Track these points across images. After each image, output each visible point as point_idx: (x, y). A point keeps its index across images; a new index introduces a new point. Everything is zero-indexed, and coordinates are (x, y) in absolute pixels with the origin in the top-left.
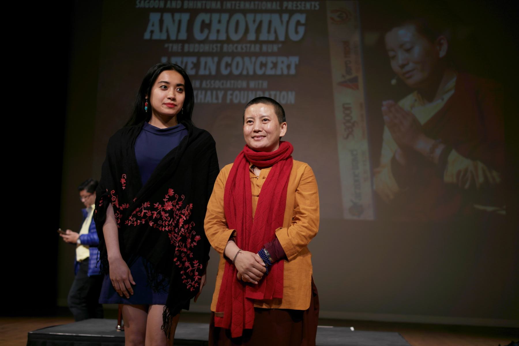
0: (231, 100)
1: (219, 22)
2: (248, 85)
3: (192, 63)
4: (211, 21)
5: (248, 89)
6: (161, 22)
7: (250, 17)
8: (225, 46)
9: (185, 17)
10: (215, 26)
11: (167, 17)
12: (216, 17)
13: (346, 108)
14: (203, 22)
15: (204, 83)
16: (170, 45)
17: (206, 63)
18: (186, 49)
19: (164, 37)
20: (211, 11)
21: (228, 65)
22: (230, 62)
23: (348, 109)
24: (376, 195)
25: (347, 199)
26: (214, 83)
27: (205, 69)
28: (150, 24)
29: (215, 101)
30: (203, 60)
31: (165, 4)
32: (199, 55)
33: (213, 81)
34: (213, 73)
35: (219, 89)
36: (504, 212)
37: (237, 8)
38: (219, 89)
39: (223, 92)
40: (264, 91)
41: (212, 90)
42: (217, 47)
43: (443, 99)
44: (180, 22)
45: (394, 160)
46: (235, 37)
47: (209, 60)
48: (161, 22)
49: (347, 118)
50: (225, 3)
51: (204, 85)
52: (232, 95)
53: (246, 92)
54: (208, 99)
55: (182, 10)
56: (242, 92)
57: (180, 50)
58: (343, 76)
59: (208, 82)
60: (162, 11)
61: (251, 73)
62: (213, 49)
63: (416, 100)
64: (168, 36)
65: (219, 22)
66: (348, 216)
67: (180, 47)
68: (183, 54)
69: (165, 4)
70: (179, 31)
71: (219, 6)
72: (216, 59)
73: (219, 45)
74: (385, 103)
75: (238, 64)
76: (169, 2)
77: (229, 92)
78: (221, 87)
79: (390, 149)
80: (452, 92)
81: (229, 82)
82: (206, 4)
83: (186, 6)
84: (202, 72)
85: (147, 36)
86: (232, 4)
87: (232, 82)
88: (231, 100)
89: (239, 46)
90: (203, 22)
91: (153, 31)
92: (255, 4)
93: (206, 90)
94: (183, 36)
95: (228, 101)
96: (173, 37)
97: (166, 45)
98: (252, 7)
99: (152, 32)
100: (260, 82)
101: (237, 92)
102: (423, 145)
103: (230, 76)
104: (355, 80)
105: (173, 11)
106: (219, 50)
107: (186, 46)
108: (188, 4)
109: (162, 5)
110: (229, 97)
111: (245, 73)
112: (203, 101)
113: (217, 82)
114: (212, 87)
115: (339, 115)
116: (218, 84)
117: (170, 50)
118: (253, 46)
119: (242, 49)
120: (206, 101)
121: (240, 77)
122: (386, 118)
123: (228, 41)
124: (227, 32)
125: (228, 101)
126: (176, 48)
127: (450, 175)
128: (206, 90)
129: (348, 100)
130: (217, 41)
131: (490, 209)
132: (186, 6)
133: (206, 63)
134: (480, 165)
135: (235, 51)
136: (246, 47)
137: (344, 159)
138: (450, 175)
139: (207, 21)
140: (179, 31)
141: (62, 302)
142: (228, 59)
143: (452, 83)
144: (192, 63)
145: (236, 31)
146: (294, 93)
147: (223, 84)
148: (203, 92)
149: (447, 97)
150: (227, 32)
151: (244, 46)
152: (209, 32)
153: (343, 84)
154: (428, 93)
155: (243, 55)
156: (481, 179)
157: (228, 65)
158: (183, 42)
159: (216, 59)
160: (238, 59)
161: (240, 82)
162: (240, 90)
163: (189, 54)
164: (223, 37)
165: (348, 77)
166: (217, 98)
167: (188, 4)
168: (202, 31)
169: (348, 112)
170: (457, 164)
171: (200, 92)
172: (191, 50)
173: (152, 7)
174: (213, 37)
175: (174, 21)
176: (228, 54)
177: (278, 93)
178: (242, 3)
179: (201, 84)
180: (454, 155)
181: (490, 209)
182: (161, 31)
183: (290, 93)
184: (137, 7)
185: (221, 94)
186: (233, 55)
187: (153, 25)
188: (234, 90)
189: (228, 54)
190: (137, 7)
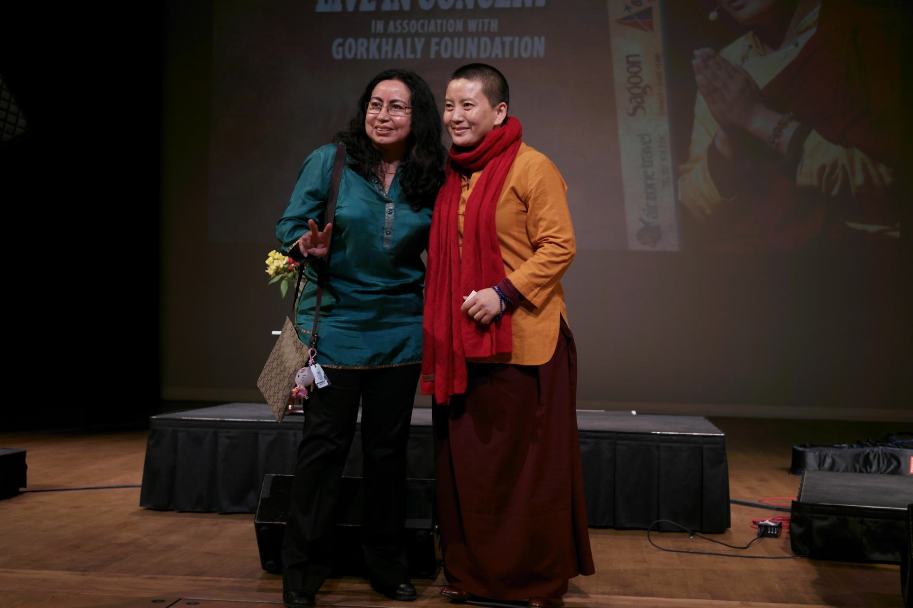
0: (438, 53)
2: (465, 26)
5: (465, 34)
13: (633, 63)
15: (391, 23)
23: (636, 64)
24: (682, 210)
25: (635, 216)
26: (408, 24)
29: (410, 56)
33: (406, 21)
34: (407, 7)
35: (417, 34)
36: (897, 234)
38: (417, 34)
39: (423, 40)
40: (492, 36)
41: (405, 36)
43: (797, 45)
45: (712, 148)
49: (634, 80)
51: (391, 28)
52: (438, 44)
53: (462, 40)
54: (399, 52)
56: (456, 40)
58: (627, 8)
59: (399, 22)
61: (470, 6)
63: (751, 47)
66: (635, 245)
74: (697, 52)
77: (434, 40)
78: (420, 31)
79: (706, 131)
80: (813, 31)
81: (433, 22)
87: (439, 22)
88: (438, 53)
93: (395, 36)
95: (432, 56)
100: (486, 21)
101: (447, 40)
102: (763, 122)
104: (648, 12)
110: (434, 48)
111: (459, 6)
112: (389, 56)
113: (413, 22)
114: (405, 31)
115: (620, 75)
116: (414, 26)
120: (395, 57)
121: (451, 13)
122: (699, 78)
125: (432, 56)
127: (807, 173)
128: (395, 36)
129: (637, 49)
131: (873, 228)
134: (859, 155)
137: (629, 150)
138: (807, 173)
141: (169, 392)
143: (813, 16)
146: (543, 38)
147: (423, 26)
148: (390, 40)
149: (803, 40)
153: (629, 21)
154: (770, 32)
156: (859, 179)
161: (451, 21)
162: (452, 35)
165: (635, 10)
166: (414, 50)
169: (635, 69)
170: (820, 153)
171: (384, 40)
177: (517, 39)
179: (386, 26)
180: (814, 138)
181: (873, 228)
183: (536, 38)
188: (441, 35)
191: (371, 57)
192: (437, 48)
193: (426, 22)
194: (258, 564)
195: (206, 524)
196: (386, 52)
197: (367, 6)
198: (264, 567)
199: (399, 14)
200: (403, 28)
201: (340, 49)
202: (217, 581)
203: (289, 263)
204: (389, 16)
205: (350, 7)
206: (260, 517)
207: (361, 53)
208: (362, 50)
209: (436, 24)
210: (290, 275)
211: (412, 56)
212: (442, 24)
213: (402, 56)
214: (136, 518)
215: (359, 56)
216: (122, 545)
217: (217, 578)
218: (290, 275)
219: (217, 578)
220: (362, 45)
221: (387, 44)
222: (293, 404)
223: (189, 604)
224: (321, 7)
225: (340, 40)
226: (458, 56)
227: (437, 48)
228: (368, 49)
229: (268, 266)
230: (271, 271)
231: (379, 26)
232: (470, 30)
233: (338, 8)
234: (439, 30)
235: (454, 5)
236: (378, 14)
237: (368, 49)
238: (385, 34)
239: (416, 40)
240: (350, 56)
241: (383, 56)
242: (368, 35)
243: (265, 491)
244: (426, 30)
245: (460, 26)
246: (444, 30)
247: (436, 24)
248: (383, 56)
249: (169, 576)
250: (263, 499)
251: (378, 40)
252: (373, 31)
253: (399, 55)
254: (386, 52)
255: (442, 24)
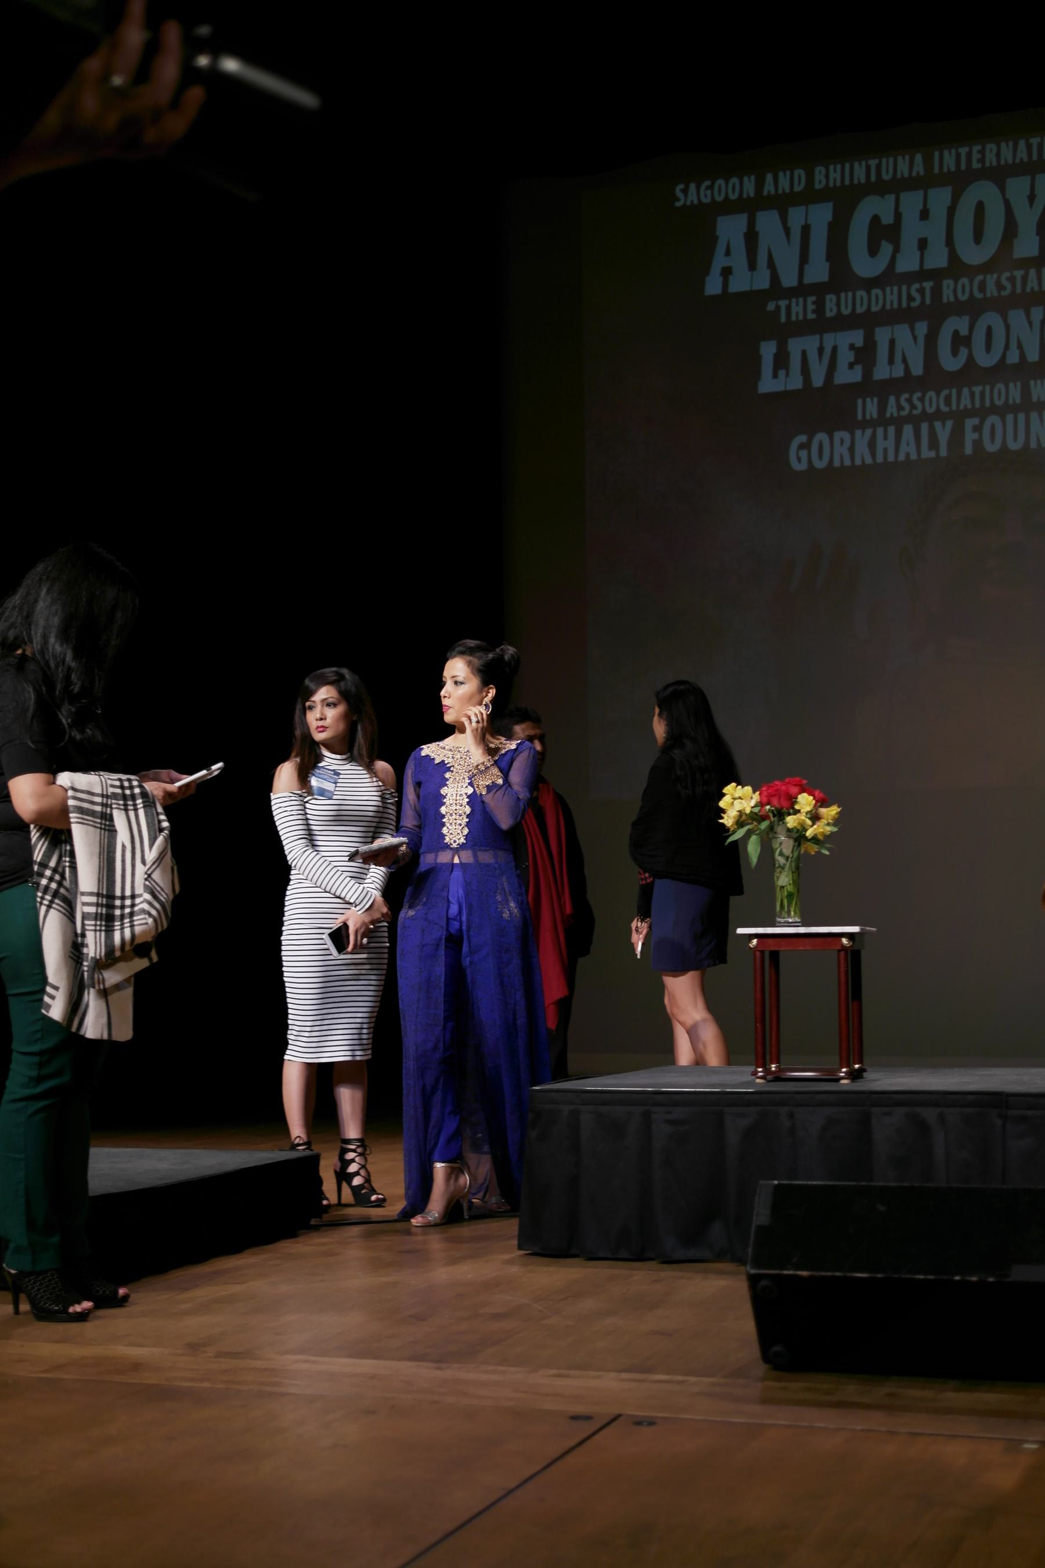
1: (924, 215)
2: (1026, 392)
3: (852, 347)
4: (898, 216)
6: (751, 238)
7: (1018, 187)
8: (948, 284)
9: (821, 215)
10: (911, 230)
11: (768, 222)
12: (911, 202)
14: (875, 220)
15: (892, 400)
16: (783, 303)
17: (892, 343)
18: (830, 311)
19: (762, 281)
20: (897, 186)
21: (959, 341)
22: (964, 332)
26: (922, 400)
27: (891, 361)
28: (720, 249)
29: (927, 454)
30: (882, 335)
31: (760, 185)
32: (868, 322)
34: (917, 370)
35: (939, 415)
37: (976, 165)
38: (939, 415)
39: (949, 424)
41: (915, 421)
42: (922, 291)
44: (806, 230)
46: (973, 255)
47: (902, 332)
48: (751, 238)
50: (937, 154)
51: (891, 409)
52: (978, 429)
53: (1021, 417)
54: (908, 448)
55: (810, 196)
56: (1010, 418)
57: (811, 316)
60: (750, 207)
62: (911, 298)
64: (775, 278)
65: (924, 215)
67: (811, 307)
68: (821, 325)
69: (760, 185)
70: (804, 258)
71: (919, 168)
72: (922, 328)
73: (928, 285)
75: (989, 331)
76: (769, 177)
77: (970, 423)
78: (944, 409)
81: (966, 391)
82: (879, 167)
83: (820, 181)
84: (882, 372)
85: (713, 286)
86: (958, 156)
87: (977, 389)
88: (978, 444)
89: (991, 280)
90: (875, 220)
91: (732, 269)
92: (1029, 147)
93: (899, 423)
94: (819, 271)
95: (968, 450)
96: (789, 280)
97: (771, 306)
98: (1022, 154)
99: (726, 272)
101: (993, 419)
103: (970, 373)
105: (782, 203)
106: (928, 301)
107: (830, 300)
108: (827, 176)
109: (749, 186)
110: (970, 437)
111: (1013, 358)
112: (891, 458)
113: (931, 394)
116: (933, 401)
117: (783, 319)
118: (1032, 272)
119: (1000, 287)
120: (902, 457)
121: (1000, 371)
123: (956, 267)
124: (950, 242)
125: (968, 450)
126: (800, 309)
128: (899, 423)
130: (922, 275)
132: (820, 181)
133: (892, 343)
135: (978, 295)
136: (1012, 280)
139: (888, 219)
140: (804, 258)
142: (959, 324)
144: (852, 347)
145: (978, 237)
147: (948, 401)
148: (891, 430)
150: (950, 242)
151: (1007, 274)
152: (896, 250)
155: (1001, 306)
157: (959, 341)
158: (819, 290)
159: (922, 328)
160: (991, 319)
161: (1000, 386)
162: (1001, 411)
163: (841, 323)
164: (937, 259)
166: (934, 444)
167: (827, 176)
168: (873, 250)
171: (880, 431)
172: (846, 311)
173: (719, 199)
174: (908, 263)
175: (787, 231)
176: (959, 308)
178: (991, 147)
179: (882, 407)
182: (752, 265)
184: (678, 204)
185: (944, 431)
186: (973, 309)
187: (728, 253)
188: (983, 413)
189: (959, 308)
190: (678, 204)
191: (858, 462)
192: (976, 436)
193: (954, 391)
194: (752, 1350)
195: (639, 1279)
196: (885, 450)
197: (847, 375)
198: (766, 1357)
199: (906, 383)
200: (913, 407)
201: (804, 454)
202: (682, 1382)
203: (761, 804)
204: (891, 387)
205: (818, 380)
206: (757, 1263)
207: (841, 455)
208: (841, 452)
209: (972, 395)
210: (764, 825)
211: (932, 454)
212: (982, 394)
213: (914, 456)
214: (515, 1269)
215: (837, 463)
216: (496, 1317)
217: (680, 1378)
218: (764, 825)
219: (680, 1378)
220: (842, 441)
221: (886, 438)
222: (778, 1062)
223: (639, 1423)
224: (768, 384)
225: (802, 438)
226: (1014, 446)
227: (976, 436)
228: (852, 450)
229: (723, 811)
230: (728, 820)
231: (872, 408)
232: (1035, 399)
233: (796, 383)
234: (977, 405)
235: (1004, 357)
236: (867, 387)
237: (852, 450)
238: (882, 420)
239: (938, 425)
240: (820, 464)
241: (880, 459)
242: (851, 425)
243: (761, 1215)
244: (954, 408)
245: (1015, 393)
246: (987, 404)
247: (972, 395)
248: (880, 459)
249: (591, 1373)
250: (759, 1228)
251: (869, 432)
252: (860, 417)
253: (908, 454)
254: (885, 450)
255: (982, 394)
